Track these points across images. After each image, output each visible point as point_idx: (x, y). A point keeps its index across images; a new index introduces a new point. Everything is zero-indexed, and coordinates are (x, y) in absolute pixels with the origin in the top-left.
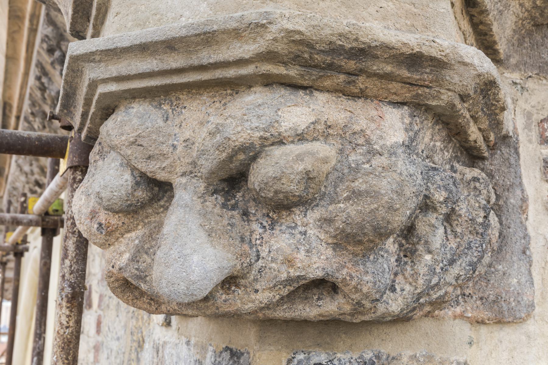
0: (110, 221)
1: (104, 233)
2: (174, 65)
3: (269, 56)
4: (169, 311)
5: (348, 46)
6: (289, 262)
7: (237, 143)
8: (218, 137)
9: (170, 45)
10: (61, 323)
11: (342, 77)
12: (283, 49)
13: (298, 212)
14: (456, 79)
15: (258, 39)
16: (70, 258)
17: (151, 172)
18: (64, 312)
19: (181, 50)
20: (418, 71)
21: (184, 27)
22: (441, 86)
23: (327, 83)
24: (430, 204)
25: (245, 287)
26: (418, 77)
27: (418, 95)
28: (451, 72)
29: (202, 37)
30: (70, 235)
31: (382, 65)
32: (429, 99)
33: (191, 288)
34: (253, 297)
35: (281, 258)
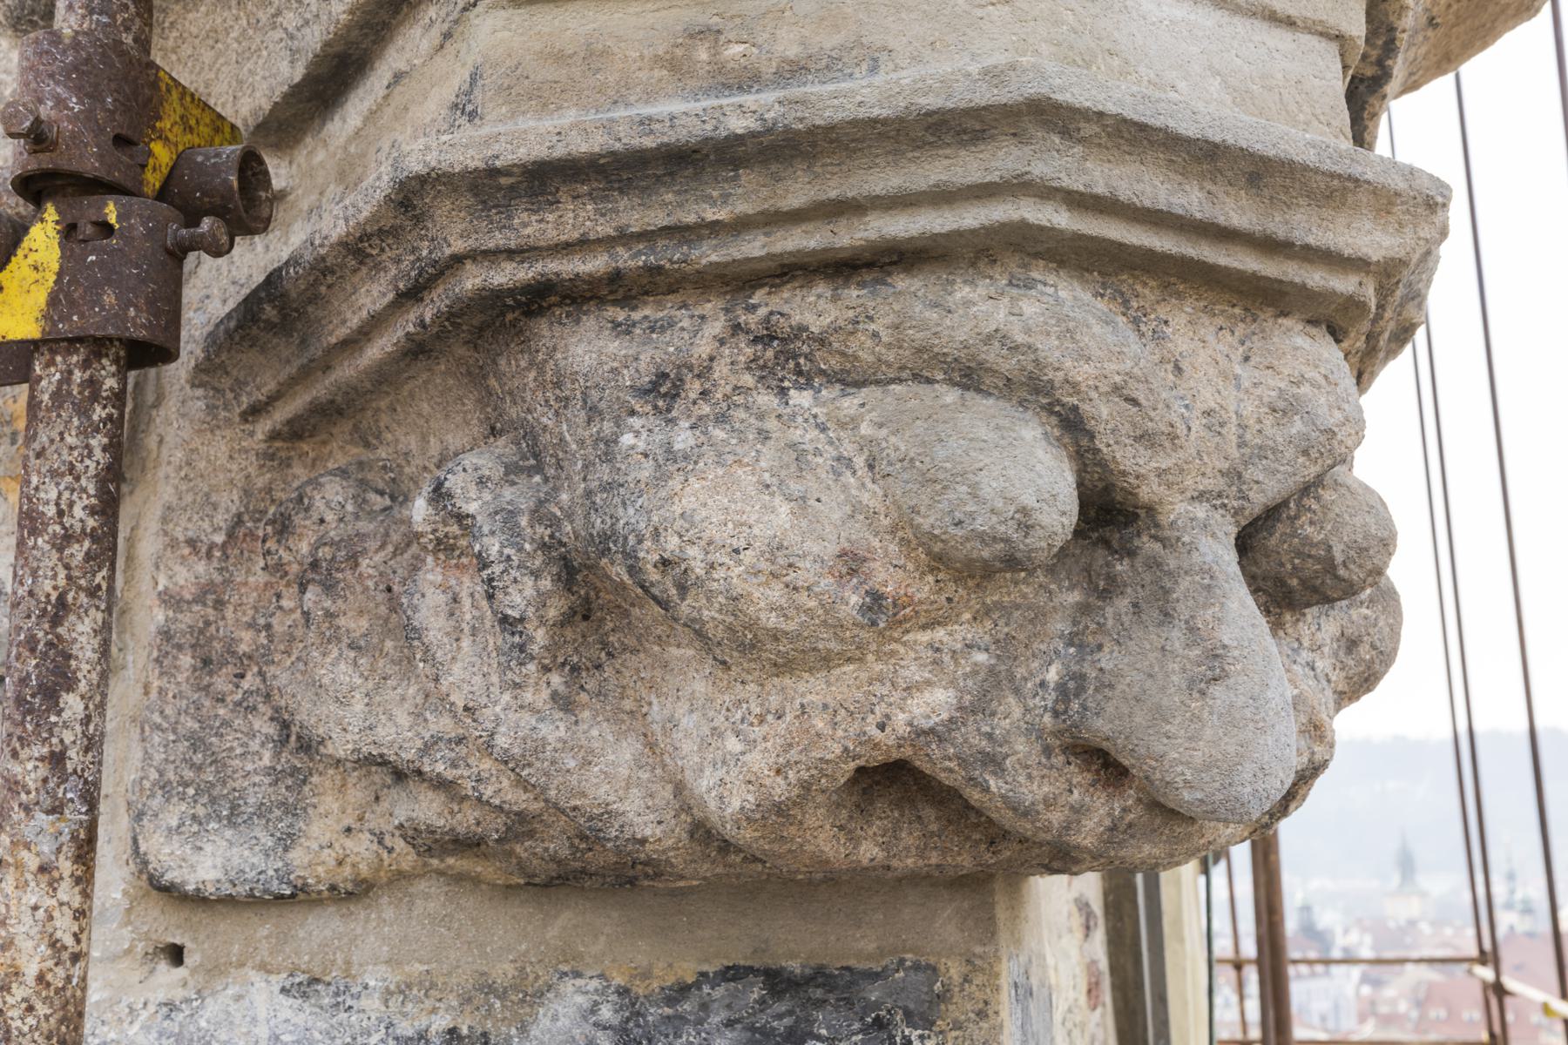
0: (910, 590)
1: (882, 625)
8: (1298, 426)
10: (53, 943)
16: (83, 686)
18: (63, 895)
30: (83, 599)
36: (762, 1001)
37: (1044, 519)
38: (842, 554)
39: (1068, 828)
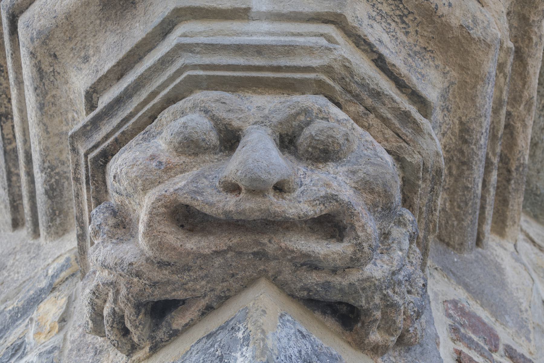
2: (257, 64)
3: (328, 70)
4: (192, 249)
5: (372, 86)
6: (328, 185)
7: (304, 105)
9: (259, 50)
11: (362, 109)
12: (337, 68)
13: (331, 166)
14: (425, 146)
15: (324, 57)
17: (229, 119)
19: (266, 56)
20: (404, 129)
21: (274, 41)
22: (414, 147)
23: (352, 109)
24: (402, 220)
25: (290, 200)
26: (404, 132)
27: (401, 147)
28: (423, 140)
29: (286, 48)
31: (386, 112)
32: (406, 154)
33: (270, 167)
34: (297, 205)
35: (321, 183)
36: (206, 342)
37: (190, 124)
38: (151, 156)
39: (224, 206)
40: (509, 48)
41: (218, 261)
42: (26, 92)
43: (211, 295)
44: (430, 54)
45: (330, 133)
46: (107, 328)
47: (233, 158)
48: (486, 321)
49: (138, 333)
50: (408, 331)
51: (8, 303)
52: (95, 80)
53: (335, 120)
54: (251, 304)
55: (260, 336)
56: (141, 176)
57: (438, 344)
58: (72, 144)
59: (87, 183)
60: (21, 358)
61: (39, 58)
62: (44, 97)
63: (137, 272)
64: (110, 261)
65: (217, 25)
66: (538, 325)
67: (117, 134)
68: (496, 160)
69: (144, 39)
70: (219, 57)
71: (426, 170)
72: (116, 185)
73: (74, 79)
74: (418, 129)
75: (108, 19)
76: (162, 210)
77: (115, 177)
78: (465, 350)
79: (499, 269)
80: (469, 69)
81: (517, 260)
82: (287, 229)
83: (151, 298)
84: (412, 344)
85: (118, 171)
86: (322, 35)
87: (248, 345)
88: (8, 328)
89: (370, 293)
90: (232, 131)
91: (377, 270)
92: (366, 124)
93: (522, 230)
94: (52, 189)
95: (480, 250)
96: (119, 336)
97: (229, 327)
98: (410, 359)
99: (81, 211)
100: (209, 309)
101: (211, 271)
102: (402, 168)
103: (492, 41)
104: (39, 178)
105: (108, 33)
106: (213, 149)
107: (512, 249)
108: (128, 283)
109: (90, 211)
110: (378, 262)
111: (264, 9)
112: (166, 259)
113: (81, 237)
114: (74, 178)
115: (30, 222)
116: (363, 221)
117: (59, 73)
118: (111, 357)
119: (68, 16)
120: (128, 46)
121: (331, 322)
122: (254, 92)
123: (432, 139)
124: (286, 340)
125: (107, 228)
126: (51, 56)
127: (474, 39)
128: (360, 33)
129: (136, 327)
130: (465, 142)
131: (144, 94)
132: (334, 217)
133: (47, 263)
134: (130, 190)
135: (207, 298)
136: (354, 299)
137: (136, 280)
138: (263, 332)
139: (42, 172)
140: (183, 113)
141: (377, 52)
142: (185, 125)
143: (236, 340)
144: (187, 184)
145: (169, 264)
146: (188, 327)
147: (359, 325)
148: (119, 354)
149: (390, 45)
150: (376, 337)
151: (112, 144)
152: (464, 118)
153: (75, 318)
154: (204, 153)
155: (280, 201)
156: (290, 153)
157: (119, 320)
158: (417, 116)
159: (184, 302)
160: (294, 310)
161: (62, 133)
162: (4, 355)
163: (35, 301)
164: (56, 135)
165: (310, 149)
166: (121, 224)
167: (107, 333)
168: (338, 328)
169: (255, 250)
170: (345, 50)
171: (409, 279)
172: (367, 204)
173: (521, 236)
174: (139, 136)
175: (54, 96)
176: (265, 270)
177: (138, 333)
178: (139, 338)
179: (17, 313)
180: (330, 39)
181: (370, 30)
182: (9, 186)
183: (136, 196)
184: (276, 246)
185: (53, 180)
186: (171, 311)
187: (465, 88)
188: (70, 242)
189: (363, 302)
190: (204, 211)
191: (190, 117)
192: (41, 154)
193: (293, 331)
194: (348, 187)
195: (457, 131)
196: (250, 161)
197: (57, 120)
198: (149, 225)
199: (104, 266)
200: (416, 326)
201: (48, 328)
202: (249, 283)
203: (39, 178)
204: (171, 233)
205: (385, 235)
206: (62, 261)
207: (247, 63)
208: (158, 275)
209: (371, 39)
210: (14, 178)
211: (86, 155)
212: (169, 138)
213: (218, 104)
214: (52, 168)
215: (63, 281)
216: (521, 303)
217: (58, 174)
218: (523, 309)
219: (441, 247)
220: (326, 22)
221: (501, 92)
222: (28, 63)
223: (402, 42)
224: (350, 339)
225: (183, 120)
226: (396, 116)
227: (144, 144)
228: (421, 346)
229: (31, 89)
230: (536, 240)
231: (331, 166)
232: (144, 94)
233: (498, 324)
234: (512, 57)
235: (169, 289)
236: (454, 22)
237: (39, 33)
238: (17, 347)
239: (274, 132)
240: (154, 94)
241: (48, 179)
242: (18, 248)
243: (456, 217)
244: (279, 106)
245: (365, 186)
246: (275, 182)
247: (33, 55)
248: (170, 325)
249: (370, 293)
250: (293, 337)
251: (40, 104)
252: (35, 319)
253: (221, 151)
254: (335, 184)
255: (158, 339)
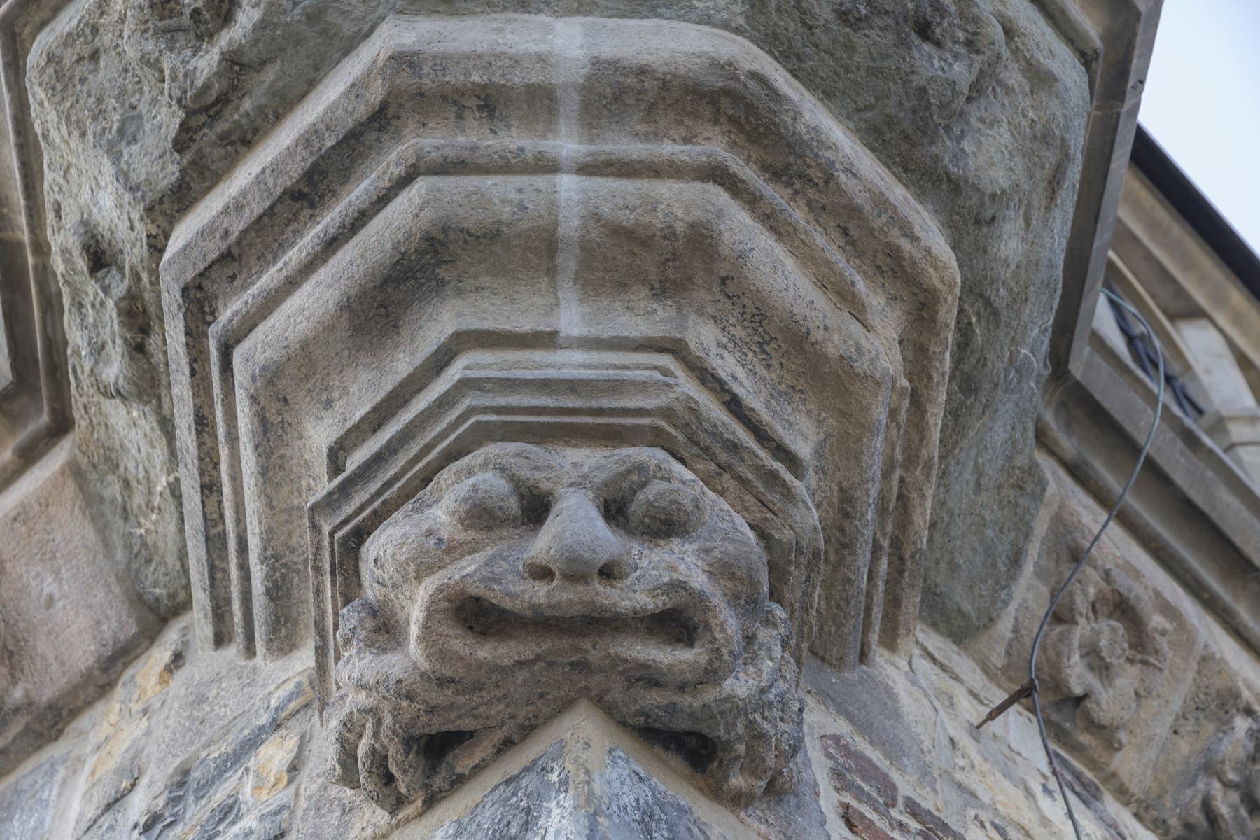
3: (667, 413)
6: (673, 568)
9: (572, 386)
11: (713, 466)
14: (798, 518)
22: (784, 519)
23: (700, 466)
25: (622, 589)
27: (766, 519)
40: (903, 388)
41: (521, 676)
42: (242, 451)
43: (512, 723)
44: (799, 395)
45: (675, 497)
46: (362, 775)
47: (542, 531)
48: (878, 764)
49: (407, 780)
50: (781, 773)
51: (212, 748)
52: (342, 433)
53: (682, 481)
54: (569, 735)
55: (582, 777)
56: (414, 559)
57: (818, 794)
58: (312, 519)
59: (333, 574)
60: (234, 823)
61: (262, 404)
62: (268, 459)
63: (408, 692)
64: (370, 679)
65: (512, 356)
66: (946, 771)
67: (376, 504)
68: (886, 543)
69: (410, 375)
70: (518, 397)
71: (799, 551)
72: (378, 572)
73: (312, 432)
74: (788, 494)
75: (359, 349)
76: (444, 605)
77: (376, 561)
78: (854, 803)
79: (891, 694)
80: (851, 416)
81: (914, 683)
82: (617, 629)
83: (427, 730)
84: (785, 793)
85: (381, 552)
86: (655, 368)
87: (566, 791)
88: (213, 783)
89: (730, 719)
90: (539, 496)
91: (740, 686)
92: (720, 488)
93: (917, 643)
94: (277, 587)
95: (865, 668)
96: (380, 785)
97: (538, 768)
98: (782, 813)
99: (322, 614)
100: (507, 745)
101: (512, 689)
102: (768, 548)
103: (882, 377)
104: (258, 572)
105: (359, 369)
106: (513, 521)
107: (907, 668)
108: (394, 709)
109: (336, 614)
110: (741, 675)
111: (576, 332)
112: (448, 674)
113: (321, 651)
114: (313, 568)
115: (242, 636)
116: (722, 617)
117: (290, 425)
118: (366, 817)
119: (305, 346)
120: (388, 385)
121: (675, 760)
122: (567, 444)
123: (808, 508)
124: (618, 784)
125: (363, 633)
126: (279, 400)
127: (858, 375)
128: (707, 365)
129: (405, 771)
130: (847, 516)
131: (414, 449)
132: (681, 612)
133: (267, 691)
134: (398, 579)
135: (505, 729)
136: (709, 727)
137: (405, 704)
138: (587, 772)
139: (262, 563)
140: (470, 473)
141: (730, 392)
142: (475, 488)
143: (549, 785)
144: (480, 568)
145: (453, 681)
146: (477, 770)
147: (716, 764)
148: (379, 810)
149: (746, 383)
150: (737, 781)
151: (369, 518)
152: (845, 484)
153: (311, 765)
154: (501, 527)
155: (609, 590)
156: (618, 526)
157: (379, 762)
158: (787, 477)
159: (471, 734)
160: (626, 744)
161: (292, 509)
162: (208, 820)
163: (252, 743)
164: (284, 511)
165: (647, 520)
166: (384, 628)
167: (362, 781)
168: (687, 770)
169: (574, 659)
170: (687, 386)
171: (783, 700)
172: (725, 595)
173: (917, 651)
174: (408, 507)
175: (282, 457)
176: (587, 688)
177: (407, 780)
178: (408, 786)
179: (226, 761)
180: (665, 372)
181: (720, 362)
182: (212, 586)
183: (406, 587)
184: (603, 653)
185: (278, 574)
186: (452, 748)
187: (845, 442)
188: (304, 659)
189: (722, 732)
190: (504, 604)
191: (481, 476)
192: (261, 538)
193: (627, 772)
194: (700, 572)
195: (836, 501)
196: (568, 534)
197: (285, 490)
198: (426, 626)
199: (361, 686)
200: (791, 765)
201: (272, 780)
202: (564, 706)
203: (258, 572)
204: (456, 637)
205: (750, 639)
206: (290, 687)
207: (556, 404)
208: (436, 697)
209: (722, 374)
210: (219, 575)
211: (332, 534)
212: (452, 506)
213: (518, 459)
214: (277, 557)
215: (292, 715)
216: (922, 742)
217: (285, 565)
218: (925, 749)
219: (814, 663)
220: (661, 350)
221: (894, 449)
222: (247, 410)
223: (763, 379)
224: (702, 785)
225: (472, 481)
226: (759, 477)
227: (416, 517)
228: (796, 796)
229: (250, 447)
230: (936, 656)
231: (676, 544)
232: (414, 449)
233: (893, 769)
234: (907, 401)
235: (452, 715)
236: (832, 351)
237: (264, 368)
238: (226, 809)
239: (597, 497)
240: (428, 448)
241: (271, 573)
242: (224, 672)
243: (834, 621)
244: (603, 461)
245: (723, 570)
246: (601, 564)
247: (254, 399)
248: (452, 768)
249: (730, 719)
250: (628, 781)
251: (262, 467)
252: (253, 768)
253: (523, 524)
254: (682, 567)
255: (435, 788)
